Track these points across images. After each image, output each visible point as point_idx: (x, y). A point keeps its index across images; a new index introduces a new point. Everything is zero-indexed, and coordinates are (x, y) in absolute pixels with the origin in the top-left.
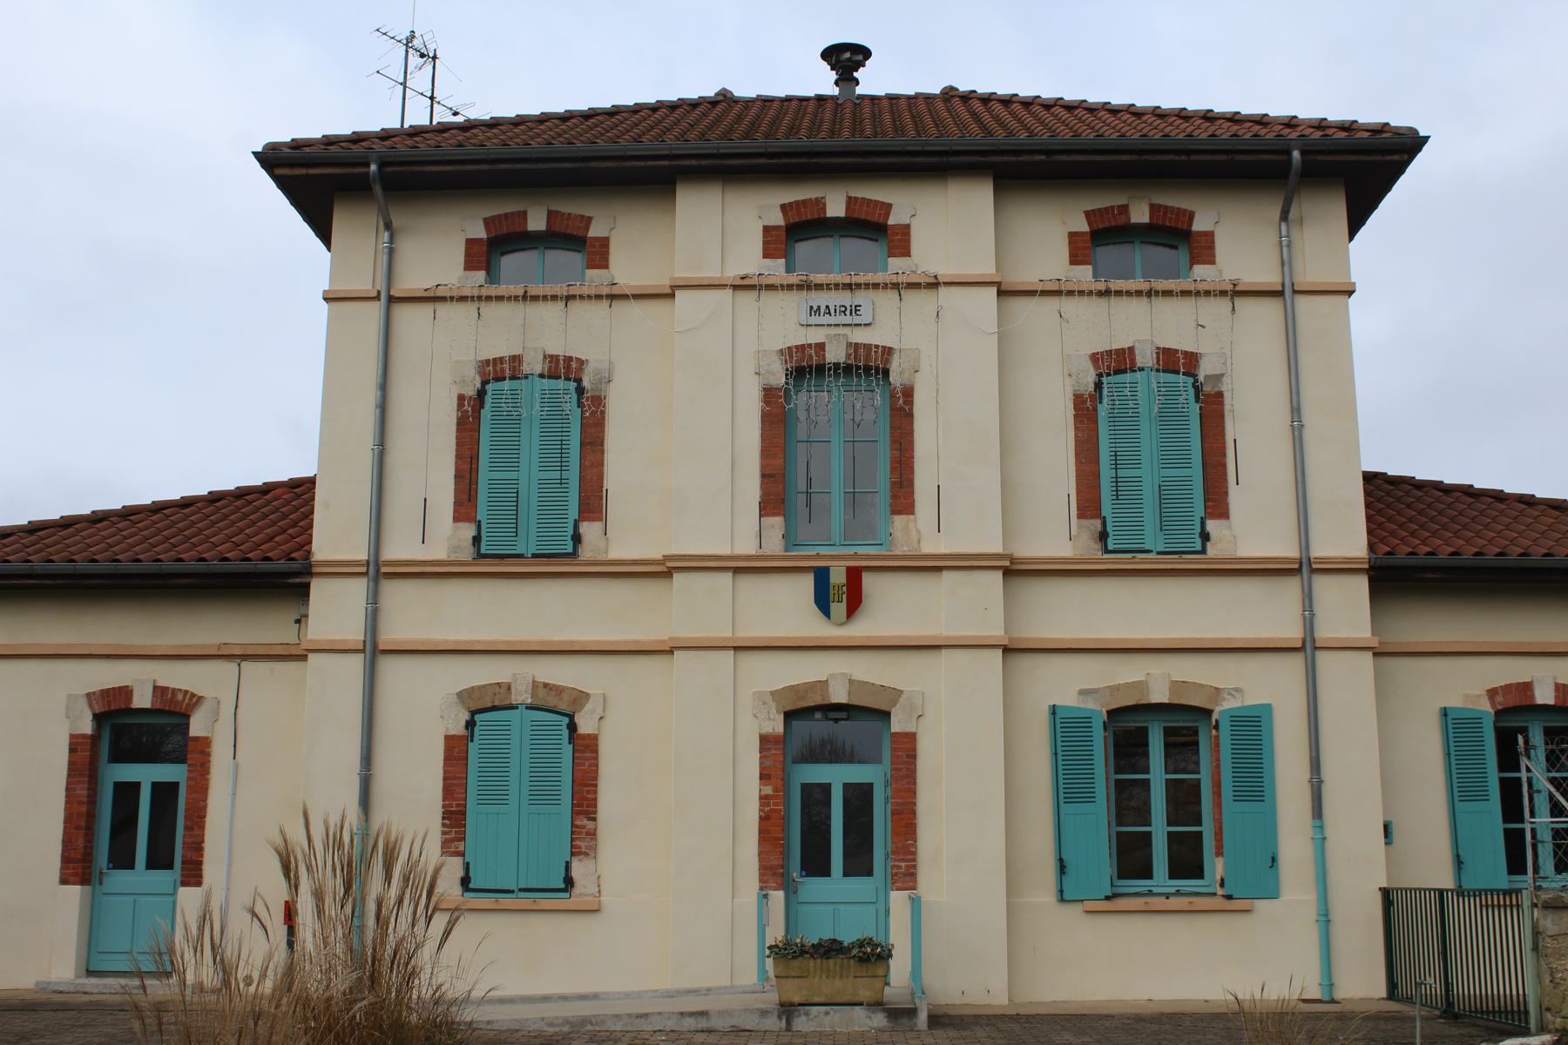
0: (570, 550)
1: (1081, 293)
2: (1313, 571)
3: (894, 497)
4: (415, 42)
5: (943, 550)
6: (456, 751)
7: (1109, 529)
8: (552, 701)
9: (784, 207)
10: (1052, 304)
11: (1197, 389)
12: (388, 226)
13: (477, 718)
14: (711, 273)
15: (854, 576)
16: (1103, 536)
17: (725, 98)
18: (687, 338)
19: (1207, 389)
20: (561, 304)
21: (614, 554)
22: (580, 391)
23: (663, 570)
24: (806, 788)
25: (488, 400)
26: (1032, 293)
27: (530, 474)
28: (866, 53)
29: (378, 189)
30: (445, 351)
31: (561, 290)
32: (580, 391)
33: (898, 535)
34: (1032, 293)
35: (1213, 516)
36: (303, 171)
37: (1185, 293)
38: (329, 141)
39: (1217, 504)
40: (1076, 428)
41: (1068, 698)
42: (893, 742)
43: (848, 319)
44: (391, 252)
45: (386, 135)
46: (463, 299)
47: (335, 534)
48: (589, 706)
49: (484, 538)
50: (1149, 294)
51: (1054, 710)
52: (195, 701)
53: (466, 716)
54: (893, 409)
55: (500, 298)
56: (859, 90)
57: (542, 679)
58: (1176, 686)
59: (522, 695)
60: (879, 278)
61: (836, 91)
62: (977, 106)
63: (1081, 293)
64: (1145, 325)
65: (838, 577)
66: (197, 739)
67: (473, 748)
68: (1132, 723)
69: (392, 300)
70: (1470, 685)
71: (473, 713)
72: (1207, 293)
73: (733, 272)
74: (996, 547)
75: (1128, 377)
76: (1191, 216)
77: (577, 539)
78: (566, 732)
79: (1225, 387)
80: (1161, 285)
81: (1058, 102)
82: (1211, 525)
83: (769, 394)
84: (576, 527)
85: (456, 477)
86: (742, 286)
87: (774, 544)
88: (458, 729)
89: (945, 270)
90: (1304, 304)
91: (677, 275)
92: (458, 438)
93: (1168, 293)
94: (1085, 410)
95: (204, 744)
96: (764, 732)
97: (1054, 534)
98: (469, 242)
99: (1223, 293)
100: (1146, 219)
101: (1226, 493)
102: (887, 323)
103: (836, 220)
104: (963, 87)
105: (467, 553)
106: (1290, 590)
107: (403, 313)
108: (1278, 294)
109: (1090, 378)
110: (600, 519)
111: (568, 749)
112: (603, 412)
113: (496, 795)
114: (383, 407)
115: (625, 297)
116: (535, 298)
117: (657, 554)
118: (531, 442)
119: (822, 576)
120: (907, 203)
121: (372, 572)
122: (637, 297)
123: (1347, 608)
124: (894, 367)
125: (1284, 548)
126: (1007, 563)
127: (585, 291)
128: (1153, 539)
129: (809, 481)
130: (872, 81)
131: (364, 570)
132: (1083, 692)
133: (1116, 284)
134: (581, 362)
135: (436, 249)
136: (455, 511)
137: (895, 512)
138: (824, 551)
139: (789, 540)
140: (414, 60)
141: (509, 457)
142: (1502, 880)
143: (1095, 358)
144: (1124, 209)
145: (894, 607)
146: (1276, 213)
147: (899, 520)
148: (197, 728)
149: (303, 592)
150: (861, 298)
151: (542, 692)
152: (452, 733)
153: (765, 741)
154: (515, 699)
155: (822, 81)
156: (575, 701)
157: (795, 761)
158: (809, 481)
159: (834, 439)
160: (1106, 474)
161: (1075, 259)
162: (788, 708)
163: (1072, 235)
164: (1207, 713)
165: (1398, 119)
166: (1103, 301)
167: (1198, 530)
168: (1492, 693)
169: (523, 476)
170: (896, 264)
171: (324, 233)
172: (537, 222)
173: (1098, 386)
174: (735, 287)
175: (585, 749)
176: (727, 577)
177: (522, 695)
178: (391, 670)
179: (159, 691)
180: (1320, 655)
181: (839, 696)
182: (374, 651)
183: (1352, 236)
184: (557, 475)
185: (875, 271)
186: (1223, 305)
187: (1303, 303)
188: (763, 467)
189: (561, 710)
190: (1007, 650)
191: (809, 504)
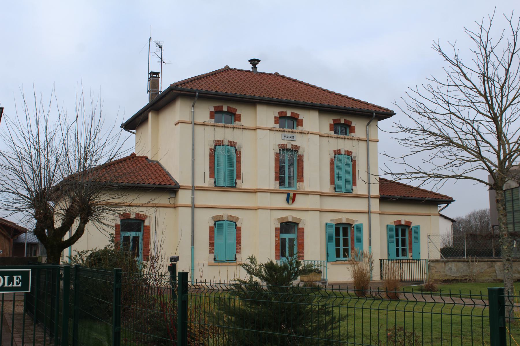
6: (212, 230)
8: (232, 219)
10: (327, 139)
11: (352, 159)
14: (264, 126)
16: (335, 188)
17: (227, 69)
20: (232, 129)
23: (254, 192)
24: (282, 239)
46: (212, 126)
51: (327, 224)
52: (146, 217)
53: (213, 222)
56: (258, 70)
58: (347, 219)
61: (251, 70)
65: (291, 195)
67: (216, 229)
69: (195, 124)
70: (391, 220)
71: (216, 222)
75: (340, 156)
76: (351, 122)
77: (236, 183)
79: (356, 159)
82: (354, 187)
86: (271, 130)
88: (212, 225)
89: (310, 130)
91: (258, 126)
92: (210, 159)
95: (148, 228)
97: (327, 189)
100: (343, 122)
102: (299, 141)
106: (366, 201)
109: (334, 155)
110: (240, 179)
111: (235, 230)
113: (220, 240)
114: (193, 150)
116: (227, 127)
118: (226, 160)
119: (288, 194)
120: (303, 115)
123: (375, 205)
125: (365, 193)
128: (344, 190)
130: (261, 68)
132: (331, 220)
141: (221, 164)
142: (396, 258)
143: (335, 151)
144: (340, 120)
145: (301, 202)
150: (295, 134)
151: (230, 217)
153: (276, 229)
154: (224, 219)
155: (249, 67)
160: (336, 176)
163: (330, 124)
164: (351, 225)
168: (395, 222)
172: (225, 109)
173: (335, 157)
175: (239, 230)
176: (269, 194)
177: (225, 218)
178: (197, 211)
179: (137, 214)
180: (371, 214)
181: (290, 220)
186: (357, 142)
187: (370, 143)
189: (233, 221)
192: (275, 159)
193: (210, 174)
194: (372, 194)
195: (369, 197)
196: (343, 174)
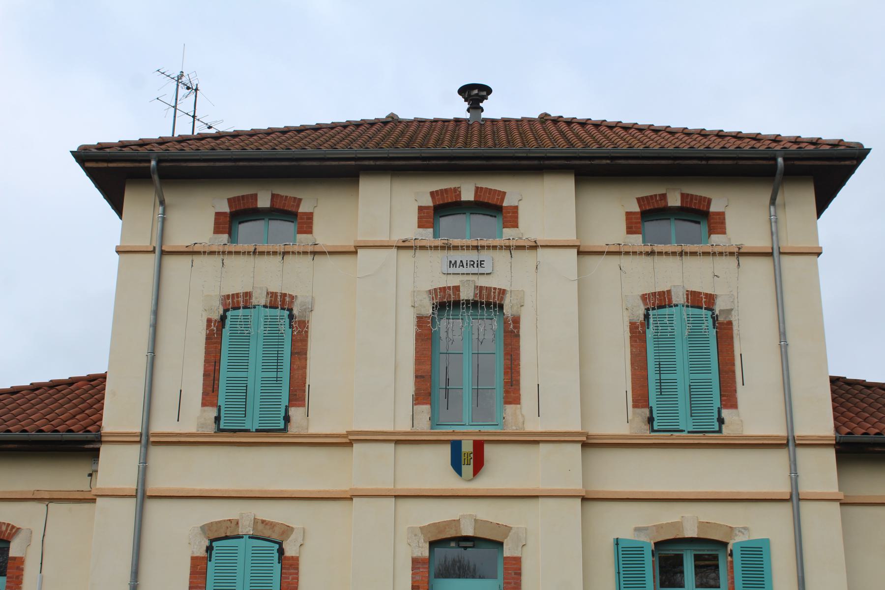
0: (282, 426)
1: (634, 253)
2: (797, 445)
3: (506, 392)
4: (184, 79)
5: (540, 429)
7: (655, 415)
8: (267, 533)
9: (432, 194)
10: (615, 260)
11: (715, 319)
12: (162, 203)
13: (214, 544)
15: (479, 447)
16: (651, 420)
17: (392, 121)
18: (364, 281)
19: (721, 319)
21: (312, 431)
22: (291, 317)
23: (346, 442)
25: (228, 322)
26: (601, 253)
27: (255, 374)
28: (489, 90)
29: (156, 177)
30: (198, 289)
31: (280, 248)
32: (291, 317)
33: (509, 418)
34: (601, 253)
35: (726, 406)
36: (105, 165)
37: (706, 254)
38: (123, 145)
39: (729, 398)
40: (631, 346)
41: (627, 534)
42: (505, 564)
43: (475, 270)
44: (164, 220)
45: (162, 141)
46: (212, 253)
47: (118, 414)
48: (293, 537)
49: (222, 418)
50: (681, 254)
53: (207, 543)
54: (505, 332)
55: (237, 253)
56: (484, 115)
57: (260, 517)
59: (246, 529)
60: (497, 242)
61: (467, 116)
62: (564, 127)
63: (634, 253)
64: (679, 275)
65: (467, 447)
66: (14, 558)
67: (211, 566)
68: (671, 551)
69: (163, 253)
71: (212, 541)
72: (721, 254)
73: (397, 237)
74: (578, 429)
75: (666, 311)
76: (709, 201)
77: (287, 419)
78: (276, 555)
79: (734, 318)
80: (689, 248)
81: (618, 124)
82: (725, 413)
83: (421, 321)
84: (287, 411)
85: (204, 375)
86: (403, 247)
87: (423, 424)
88: (201, 552)
89: (542, 237)
90: (787, 262)
93: (694, 254)
94: (637, 333)
96: (415, 555)
97: (617, 418)
98: (218, 214)
99: (732, 254)
101: (735, 391)
102: (502, 273)
103: (468, 203)
104: (554, 114)
105: (211, 428)
106: (780, 458)
107: (171, 262)
108: (771, 254)
109: (641, 311)
110: (304, 406)
111: (277, 567)
112: (307, 332)
114: (155, 326)
115: (323, 253)
116: (262, 253)
117: (345, 432)
118: (256, 351)
119: (456, 447)
120: (515, 191)
121: (143, 441)
122: (331, 253)
123: (821, 471)
124: (507, 303)
125: (778, 430)
126: (584, 439)
127: (296, 249)
128: (685, 422)
129: (447, 381)
130: (491, 109)
131: (138, 439)
132: (637, 529)
133: (658, 248)
134: (292, 297)
135: (194, 217)
136: (203, 399)
137: (507, 402)
138: (458, 429)
139: (434, 421)
140: (183, 91)
141: (241, 362)
143: (644, 298)
145: (505, 469)
146: (766, 197)
147: (510, 408)
148: (14, 550)
149: (95, 454)
150: (485, 255)
151: (260, 526)
152: (196, 555)
153: (416, 562)
154: (241, 531)
155: (459, 109)
156: (283, 533)
157: (435, 577)
158: (447, 381)
159: (465, 350)
161: (630, 230)
162: (432, 539)
163: (629, 215)
164: (725, 545)
165: (849, 138)
166: (649, 259)
167: (716, 416)
169: (250, 375)
170: (508, 232)
171: (118, 208)
172: (264, 201)
173: (647, 316)
174: (399, 247)
176: (392, 445)
177: (246, 529)
178: (154, 508)
181: (468, 531)
182: (143, 496)
183: (819, 216)
184: (274, 375)
185: (494, 238)
186: (733, 261)
187: (786, 261)
188: (416, 370)
190: (584, 499)
191: (447, 396)
192: (418, 336)
193: (205, 394)
194: (801, 431)
195: (788, 444)
196: (685, 371)
